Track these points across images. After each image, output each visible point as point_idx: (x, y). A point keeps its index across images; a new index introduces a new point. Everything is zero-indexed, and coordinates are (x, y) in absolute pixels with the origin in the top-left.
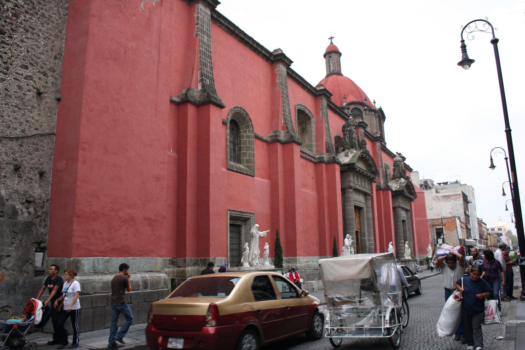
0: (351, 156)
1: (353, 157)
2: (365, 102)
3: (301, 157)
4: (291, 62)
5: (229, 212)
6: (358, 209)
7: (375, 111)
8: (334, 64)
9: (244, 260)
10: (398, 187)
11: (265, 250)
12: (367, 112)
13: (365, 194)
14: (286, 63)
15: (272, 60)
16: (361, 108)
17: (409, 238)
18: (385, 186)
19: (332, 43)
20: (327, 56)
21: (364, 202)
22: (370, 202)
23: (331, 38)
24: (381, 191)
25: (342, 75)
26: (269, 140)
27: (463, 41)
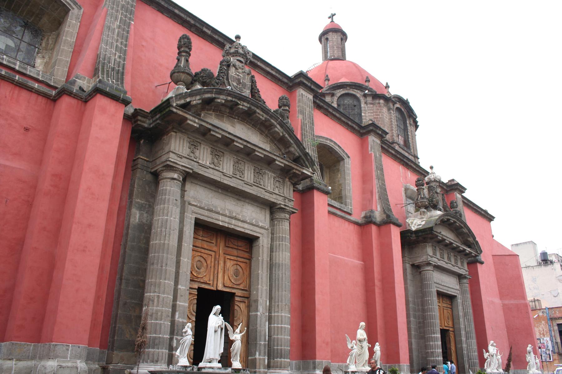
2: (367, 84)
7: (387, 100)
10: (423, 223)
12: (369, 99)
16: (358, 94)
17: (467, 333)
18: (384, 216)
19: (332, 21)
24: (374, 228)
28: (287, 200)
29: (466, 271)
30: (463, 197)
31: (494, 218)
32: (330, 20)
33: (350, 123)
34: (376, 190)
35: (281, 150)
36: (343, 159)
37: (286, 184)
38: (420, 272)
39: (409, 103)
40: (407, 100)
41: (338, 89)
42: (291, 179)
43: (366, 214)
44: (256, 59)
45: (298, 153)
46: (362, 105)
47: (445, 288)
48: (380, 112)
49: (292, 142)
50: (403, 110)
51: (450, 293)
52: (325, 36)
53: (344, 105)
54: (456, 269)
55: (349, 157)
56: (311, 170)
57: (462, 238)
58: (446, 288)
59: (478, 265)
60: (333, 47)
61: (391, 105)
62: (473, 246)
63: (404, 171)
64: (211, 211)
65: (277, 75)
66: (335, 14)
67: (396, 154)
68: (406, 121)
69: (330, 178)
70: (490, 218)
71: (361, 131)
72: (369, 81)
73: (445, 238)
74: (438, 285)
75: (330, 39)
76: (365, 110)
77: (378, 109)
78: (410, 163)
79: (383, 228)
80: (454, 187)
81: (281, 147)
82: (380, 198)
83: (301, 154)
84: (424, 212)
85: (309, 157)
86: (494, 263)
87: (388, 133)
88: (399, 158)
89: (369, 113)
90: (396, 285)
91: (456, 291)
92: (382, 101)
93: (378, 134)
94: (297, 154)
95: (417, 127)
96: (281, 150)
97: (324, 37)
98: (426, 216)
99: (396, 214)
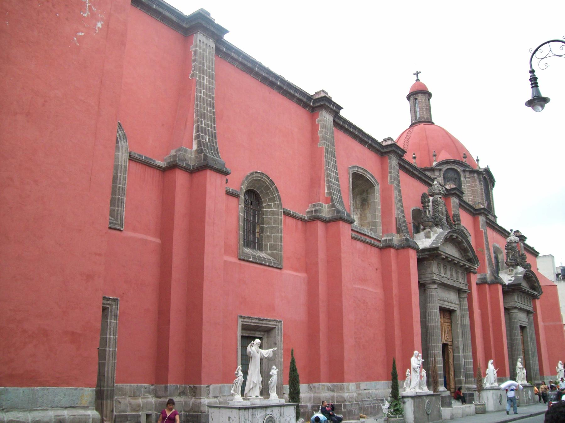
0: (433, 237)
1: (437, 238)
2: (464, 160)
3: (354, 238)
4: (340, 108)
5: (240, 320)
6: (447, 312)
7: (478, 173)
8: (421, 109)
9: (234, 390)
10: (513, 279)
11: (272, 376)
12: (467, 174)
13: (459, 291)
14: (331, 109)
15: (311, 107)
16: (459, 169)
17: (533, 352)
18: (493, 277)
19: (418, 80)
20: (412, 98)
21: (457, 302)
22: (466, 302)
23: (417, 73)
24: (487, 286)
25: (433, 123)
26: (306, 217)
27: (532, 72)
34: (486, 258)
63: (491, 233)
64: (443, 301)
66: (420, 72)
81: (462, 252)
84: (512, 270)
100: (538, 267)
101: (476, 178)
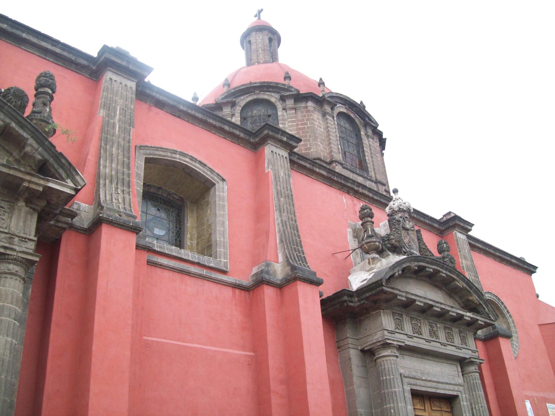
2: (287, 82)
7: (320, 101)
12: (290, 103)
16: (274, 98)
18: (288, 268)
19: (259, 18)
28: (17, 239)
29: (473, 351)
30: (470, 237)
31: (536, 268)
32: (257, 18)
33: (227, 128)
35: (11, 154)
36: (214, 184)
37: (16, 212)
38: (375, 360)
39: (364, 107)
40: (361, 102)
41: (242, 95)
42: (31, 202)
43: (258, 269)
44: (18, 29)
45: (40, 154)
46: (280, 113)
47: (429, 384)
48: (307, 120)
49: (25, 135)
50: (352, 115)
51: (442, 392)
52: (248, 39)
53: (252, 117)
54: (450, 350)
55: (223, 180)
56: (71, 184)
57: (461, 298)
58: (434, 384)
59: (503, 342)
60: (257, 51)
61: (328, 108)
62: (480, 309)
63: (350, 202)
65: (65, 54)
66: (262, 10)
67: (330, 175)
68: (360, 131)
69: (197, 218)
70: (530, 269)
71: (252, 140)
72: (290, 78)
73: (413, 297)
74: (412, 381)
75: (253, 41)
76: (283, 120)
77: (305, 116)
78: (360, 190)
79: (287, 291)
80: (454, 223)
82: (282, 241)
83: (47, 156)
84: (373, 259)
85: (63, 161)
86: (543, 336)
87: (301, 140)
88: (337, 182)
89: (289, 122)
90: (309, 387)
91: (456, 388)
92: (310, 104)
93: (281, 141)
94: (39, 157)
95: (382, 143)
96: (11, 154)
97: (246, 39)
98: (379, 265)
99: (316, 264)
100: (537, 292)
101: (310, 108)
